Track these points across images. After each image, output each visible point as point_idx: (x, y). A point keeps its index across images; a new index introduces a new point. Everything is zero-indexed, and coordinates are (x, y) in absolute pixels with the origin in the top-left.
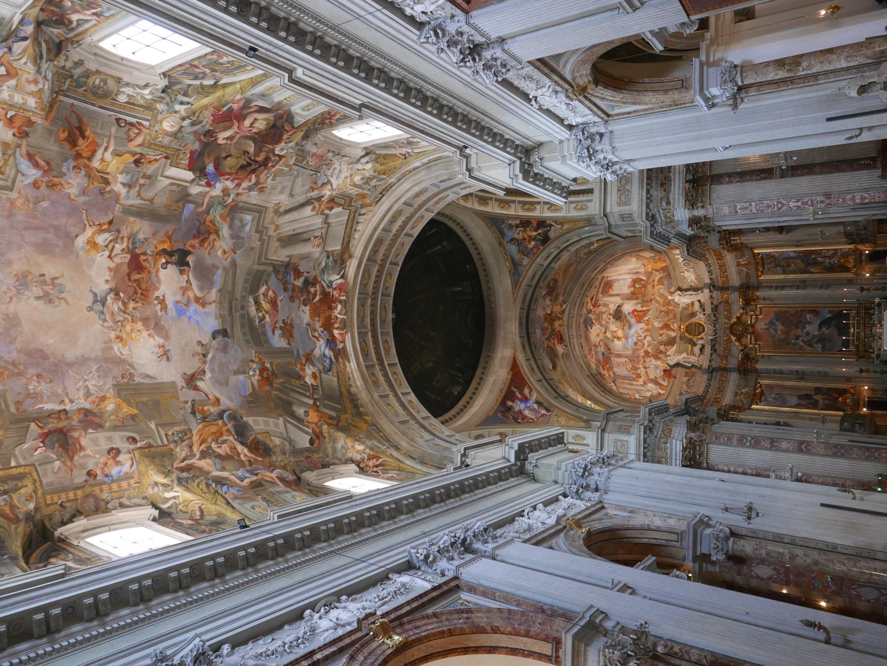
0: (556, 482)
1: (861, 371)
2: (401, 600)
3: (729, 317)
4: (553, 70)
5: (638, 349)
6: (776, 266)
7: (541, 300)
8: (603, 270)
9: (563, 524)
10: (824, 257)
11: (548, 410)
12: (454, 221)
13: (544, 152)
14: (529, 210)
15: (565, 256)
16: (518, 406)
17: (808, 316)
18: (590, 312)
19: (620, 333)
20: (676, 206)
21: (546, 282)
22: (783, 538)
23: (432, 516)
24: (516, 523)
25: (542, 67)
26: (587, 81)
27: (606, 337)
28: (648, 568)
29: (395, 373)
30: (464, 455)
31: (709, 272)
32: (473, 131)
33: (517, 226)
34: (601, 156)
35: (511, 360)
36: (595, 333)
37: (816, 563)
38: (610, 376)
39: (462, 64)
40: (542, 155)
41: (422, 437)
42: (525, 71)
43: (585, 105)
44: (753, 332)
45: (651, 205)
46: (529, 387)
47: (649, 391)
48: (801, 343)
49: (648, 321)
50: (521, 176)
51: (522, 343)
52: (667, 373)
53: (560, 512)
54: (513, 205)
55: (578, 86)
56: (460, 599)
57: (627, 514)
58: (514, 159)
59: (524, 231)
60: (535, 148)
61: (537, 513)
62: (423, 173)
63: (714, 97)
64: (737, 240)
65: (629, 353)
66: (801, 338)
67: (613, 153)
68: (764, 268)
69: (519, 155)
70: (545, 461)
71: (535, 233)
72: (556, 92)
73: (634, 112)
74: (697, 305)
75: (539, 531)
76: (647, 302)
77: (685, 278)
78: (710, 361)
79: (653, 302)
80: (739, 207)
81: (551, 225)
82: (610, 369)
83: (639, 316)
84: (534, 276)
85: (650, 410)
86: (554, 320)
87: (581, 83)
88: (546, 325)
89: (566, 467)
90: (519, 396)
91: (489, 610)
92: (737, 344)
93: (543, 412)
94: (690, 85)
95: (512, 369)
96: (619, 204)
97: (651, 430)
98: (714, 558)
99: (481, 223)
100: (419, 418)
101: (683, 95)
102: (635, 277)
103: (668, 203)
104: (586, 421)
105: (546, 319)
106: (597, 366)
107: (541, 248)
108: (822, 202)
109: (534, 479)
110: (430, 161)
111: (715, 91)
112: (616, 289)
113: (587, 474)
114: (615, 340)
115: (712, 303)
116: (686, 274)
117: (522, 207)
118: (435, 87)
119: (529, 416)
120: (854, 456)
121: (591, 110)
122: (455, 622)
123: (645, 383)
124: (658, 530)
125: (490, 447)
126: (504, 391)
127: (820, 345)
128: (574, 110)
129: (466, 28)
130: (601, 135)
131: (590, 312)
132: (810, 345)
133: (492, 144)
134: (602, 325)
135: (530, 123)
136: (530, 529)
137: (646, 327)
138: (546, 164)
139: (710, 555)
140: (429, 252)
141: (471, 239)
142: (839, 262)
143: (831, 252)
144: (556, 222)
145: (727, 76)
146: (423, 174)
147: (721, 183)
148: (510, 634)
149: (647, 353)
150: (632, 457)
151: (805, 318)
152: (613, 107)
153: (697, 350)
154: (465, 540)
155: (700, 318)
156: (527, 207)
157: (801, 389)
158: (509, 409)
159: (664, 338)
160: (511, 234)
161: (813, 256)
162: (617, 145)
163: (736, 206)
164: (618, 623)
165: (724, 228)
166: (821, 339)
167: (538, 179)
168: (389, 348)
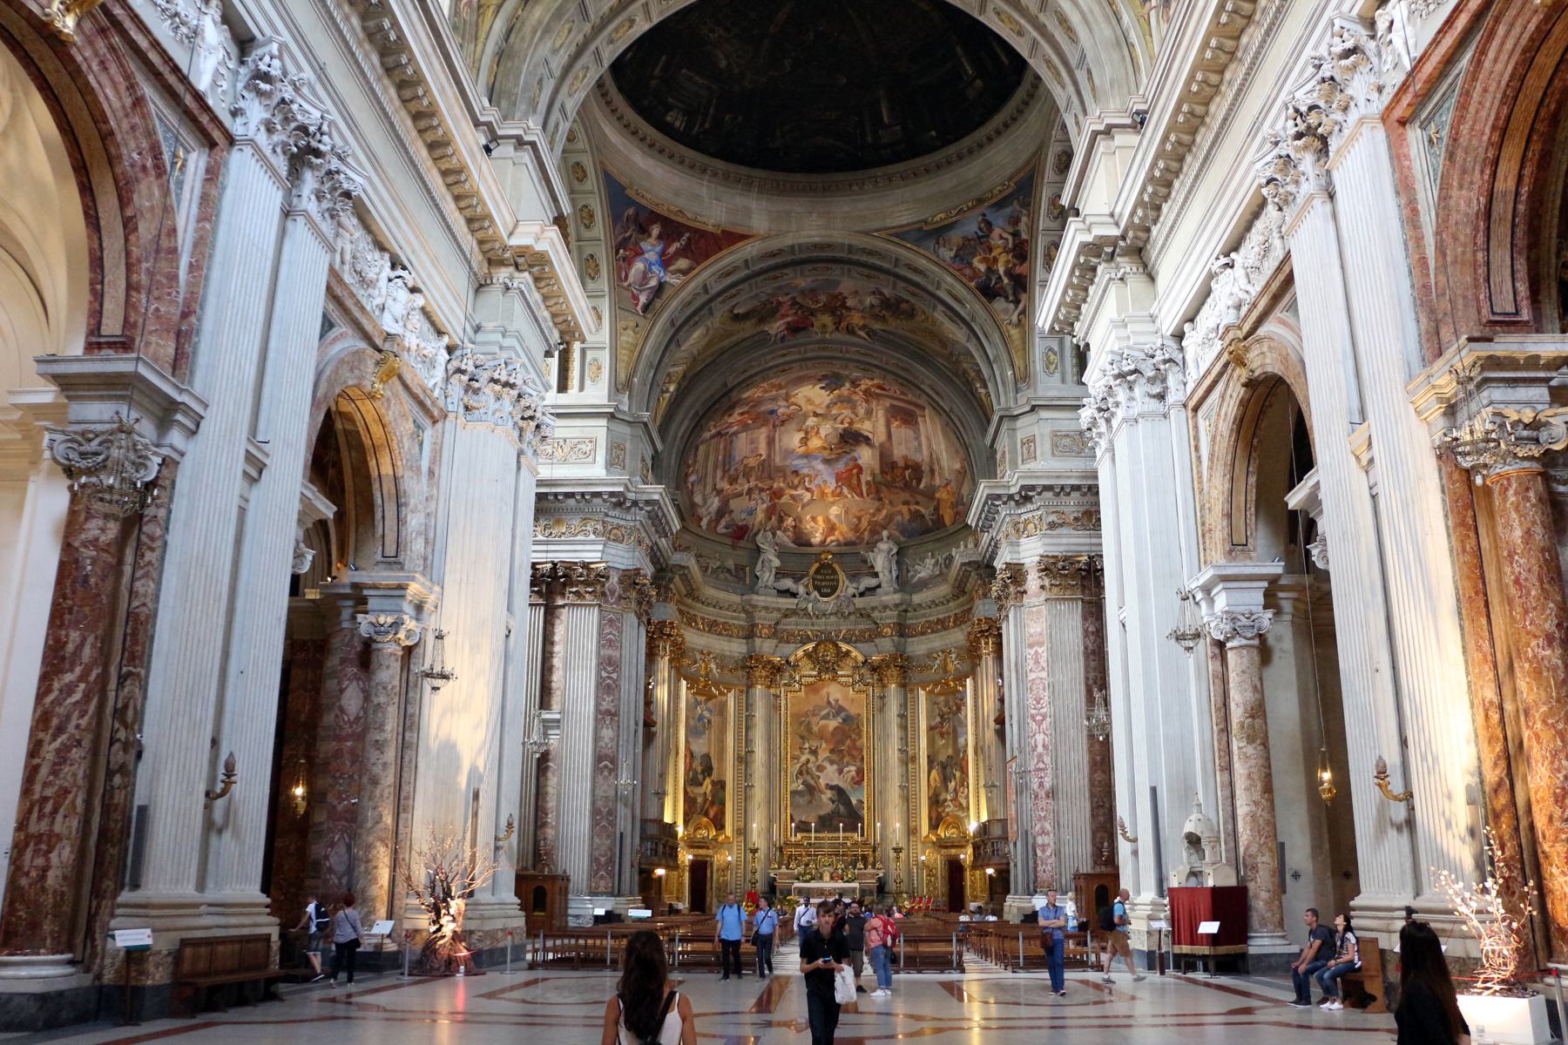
0: (477, 329)
1: (754, 851)
2: (162, 30)
4: (1276, 299)
5: (785, 477)
6: (942, 717)
7: (872, 286)
8: (937, 409)
9: (387, 346)
10: (955, 789)
11: (646, 308)
12: (1026, 103)
13: (1136, 282)
15: (958, 334)
16: (651, 248)
17: (853, 768)
18: (855, 384)
19: (815, 443)
20: (1047, 540)
21: (905, 296)
22: (411, 729)
23: (368, 82)
24: (377, 255)
25: (1281, 277)
26: (1253, 366)
27: (806, 417)
28: (306, 505)
30: (520, 142)
31: (933, 602)
32: (1173, 138)
33: (1016, 234)
34: (1121, 394)
35: (745, 232)
36: (812, 395)
37: (375, 782)
38: (731, 425)
39: (1291, 110)
40: (1130, 279)
41: (555, 51)
42: (1277, 243)
43: (1213, 365)
44: (821, 680)
45: (1049, 494)
46: (690, 269)
47: (705, 500)
48: (803, 759)
49: (840, 494)
50: (1089, 238)
51: (780, 252)
52: (740, 533)
53: (411, 340)
55: (1247, 349)
56: (187, 151)
57: (425, 464)
58: (1122, 225)
60: (1145, 266)
61: (403, 295)
62: (1108, 32)
63: (1211, 601)
64: (987, 649)
65: (778, 460)
66: (812, 759)
67: (1125, 420)
68: (939, 694)
69: (1131, 234)
70: (518, 306)
71: (1001, 271)
72: (1238, 307)
73: (1199, 458)
74: (872, 582)
75: (364, 301)
76: (878, 491)
77: (923, 560)
78: (766, 608)
79: (877, 504)
80: (1040, 650)
81: (1017, 302)
82: (745, 427)
83: (850, 478)
84: (916, 270)
85: (655, 502)
86: (833, 313)
87: (1251, 355)
88: (823, 298)
89: (512, 348)
90: (672, 249)
91: (168, 210)
92: (800, 653)
93: (643, 299)
94: (1235, 559)
95: (723, 231)
96: (1055, 434)
97: (619, 505)
98: (360, 617)
99: (1021, 162)
100: (597, 42)
101: (1219, 546)
102: (925, 468)
103: (1052, 526)
104: (628, 385)
105: (836, 297)
106: (746, 402)
107: (973, 284)
108: (1041, 785)
109: (480, 287)
110: (1130, 46)
111: (1221, 601)
112: (901, 432)
113: (498, 387)
114: (802, 435)
115: (873, 609)
116: (929, 562)
118: (1258, 53)
119: (633, 271)
120: (596, 840)
121: (1204, 377)
122: (132, 144)
123: (719, 492)
124: (400, 521)
125: (544, 196)
126: (680, 220)
127: (801, 787)
128: (1207, 341)
129: (1353, 115)
130: (1161, 397)
131: (855, 384)
132: (800, 772)
133: (1150, 179)
134: (828, 406)
135: (1187, 254)
136: (365, 282)
137: (828, 491)
138: (1113, 290)
139: (366, 612)
140: (959, 50)
141: (990, 140)
142: (948, 814)
144: (1023, 312)
145: (1244, 621)
146: (1105, 30)
147: (1085, 618)
148: (128, 254)
149: (777, 494)
150: (545, 472)
152: (1207, 418)
153: (787, 583)
154: (318, 153)
155: (847, 588)
157: (721, 759)
158: (644, 231)
159: (808, 526)
161: (958, 774)
162: (1140, 425)
163: (1041, 644)
164: (182, 454)
165: (1004, 626)
166: (811, 790)
167: (1085, 273)
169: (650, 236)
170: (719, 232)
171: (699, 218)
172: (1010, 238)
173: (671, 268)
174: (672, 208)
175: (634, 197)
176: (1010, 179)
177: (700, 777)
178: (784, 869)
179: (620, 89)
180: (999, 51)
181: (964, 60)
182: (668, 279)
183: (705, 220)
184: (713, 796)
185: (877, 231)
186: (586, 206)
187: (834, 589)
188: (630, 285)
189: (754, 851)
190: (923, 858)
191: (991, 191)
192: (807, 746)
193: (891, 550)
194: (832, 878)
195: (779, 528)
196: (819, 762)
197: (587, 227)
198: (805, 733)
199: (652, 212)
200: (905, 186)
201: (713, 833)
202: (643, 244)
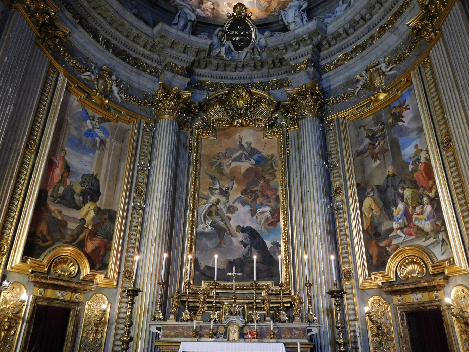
3: (262, 86)
6: (373, 137)
10: (407, 215)
17: (267, 209)
66: (223, 199)
127: (209, 229)
132: (209, 213)
142: (397, 246)
143: (427, 226)
151: (262, 205)
161: (407, 193)
177: (78, 199)
178: (172, 321)
184: (96, 226)
187: (247, 43)
189: (135, 293)
190: (367, 309)
192: (217, 186)
193: (301, 7)
194: (242, 336)
195: (199, 8)
196: (230, 203)
198: (217, 175)
201: (86, 270)
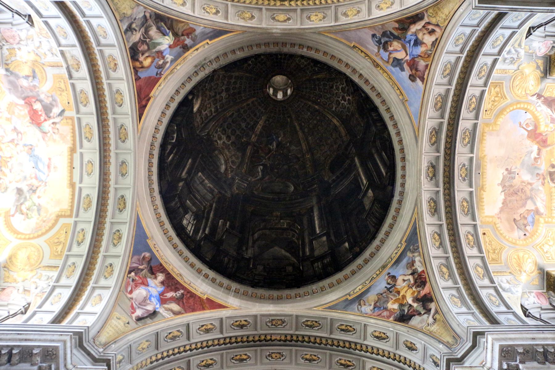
11: (139, 319)
14: (441, 271)
29: (217, 12)
54: (440, 253)
59: (410, 287)
71: (410, 300)
81: (428, 311)
90: (170, 295)
93: (139, 313)
95: (207, 299)
107: (391, 319)
117: (442, 264)
126: (178, 279)
144: (436, 312)
156: (445, 270)
158: (152, 273)
160: (401, 272)
168: (244, 18)
169: (156, 278)
170: (206, 297)
171: (192, 284)
172: (411, 278)
173: (166, 306)
174: (175, 270)
175: (152, 247)
176: (401, 241)
179: (161, 192)
180: (379, 162)
181: (360, 170)
182: (161, 310)
183: (195, 287)
185: (315, 307)
186: (118, 231)
188: (132, 298)
191: (390, 257)
197: (115, 245)
199: (161, 265)
200: (331, 292)
202: (149, 280)
